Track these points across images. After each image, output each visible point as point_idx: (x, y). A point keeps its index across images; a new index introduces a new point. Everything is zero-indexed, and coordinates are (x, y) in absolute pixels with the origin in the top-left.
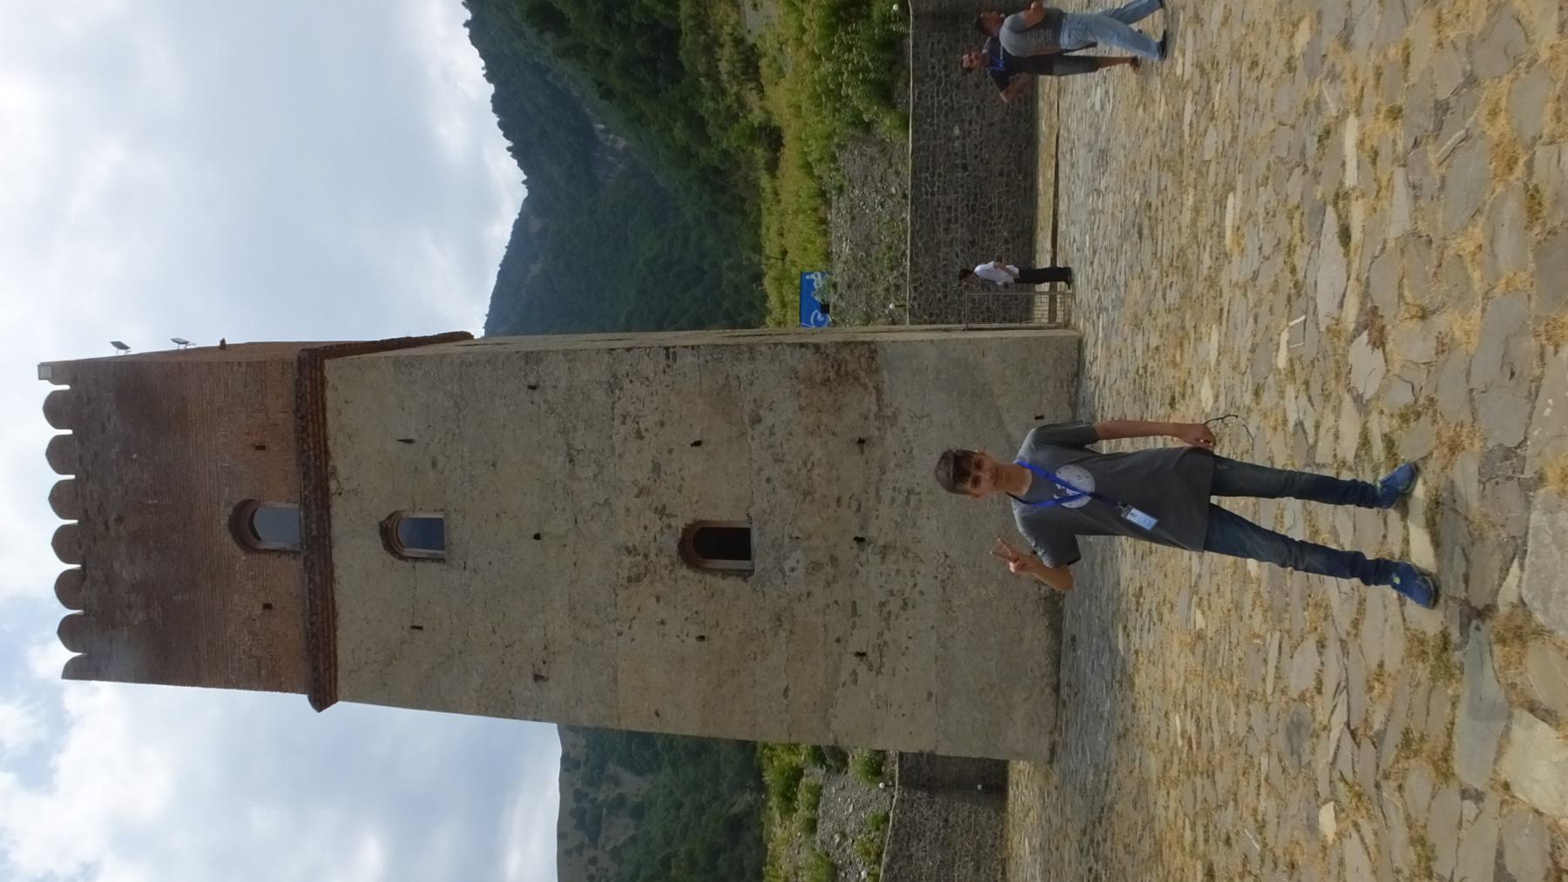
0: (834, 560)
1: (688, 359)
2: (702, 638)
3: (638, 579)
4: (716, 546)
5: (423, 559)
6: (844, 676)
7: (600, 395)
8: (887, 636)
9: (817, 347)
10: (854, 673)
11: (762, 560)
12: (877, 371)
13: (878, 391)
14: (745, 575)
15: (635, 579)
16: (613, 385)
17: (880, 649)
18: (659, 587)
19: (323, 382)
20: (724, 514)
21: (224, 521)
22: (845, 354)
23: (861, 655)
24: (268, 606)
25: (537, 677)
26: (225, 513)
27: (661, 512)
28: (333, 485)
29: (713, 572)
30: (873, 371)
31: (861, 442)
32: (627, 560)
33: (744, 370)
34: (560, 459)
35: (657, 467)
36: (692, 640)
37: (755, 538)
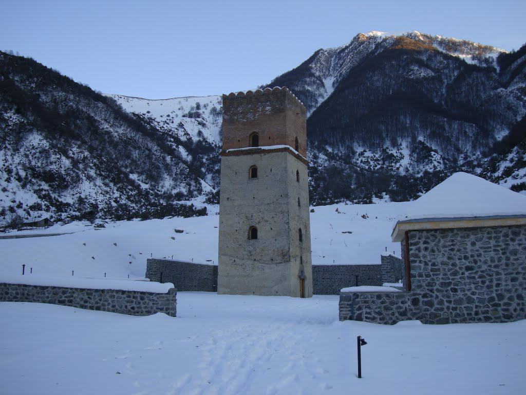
0: (251, 255)
1: (287, 227)
2: (236, 230)
3: (247, 218)
4: (253, 233)
5: (249, 174)
6: (231, 258)
7: (280, 210)
8: (238, 266)
9: (289, 251)
10: (231, 260)
11: (252, 241)
12: (285, 262)
13: (281, 263)
14: (249, 238)
15: (247, 217)
16: (282, 212)
17: (236, 264)
18: (245, 222)
19: (283, 152)
20: (259, 234)
21: (255, 131)
22: (288, 256)
23: (235, 261)
24: (239, 141)
25: (228, 198)
26: (256, 130)
27: (259, 222)
28: (263, 154)
29: (249, 232)
30: (284, 262)
31: (272, 260)
32: (250, 216)
33: (285, 237)
34: (269, 202)
35: (267, 221)
36: (236, 229)
37: (254, 240)
